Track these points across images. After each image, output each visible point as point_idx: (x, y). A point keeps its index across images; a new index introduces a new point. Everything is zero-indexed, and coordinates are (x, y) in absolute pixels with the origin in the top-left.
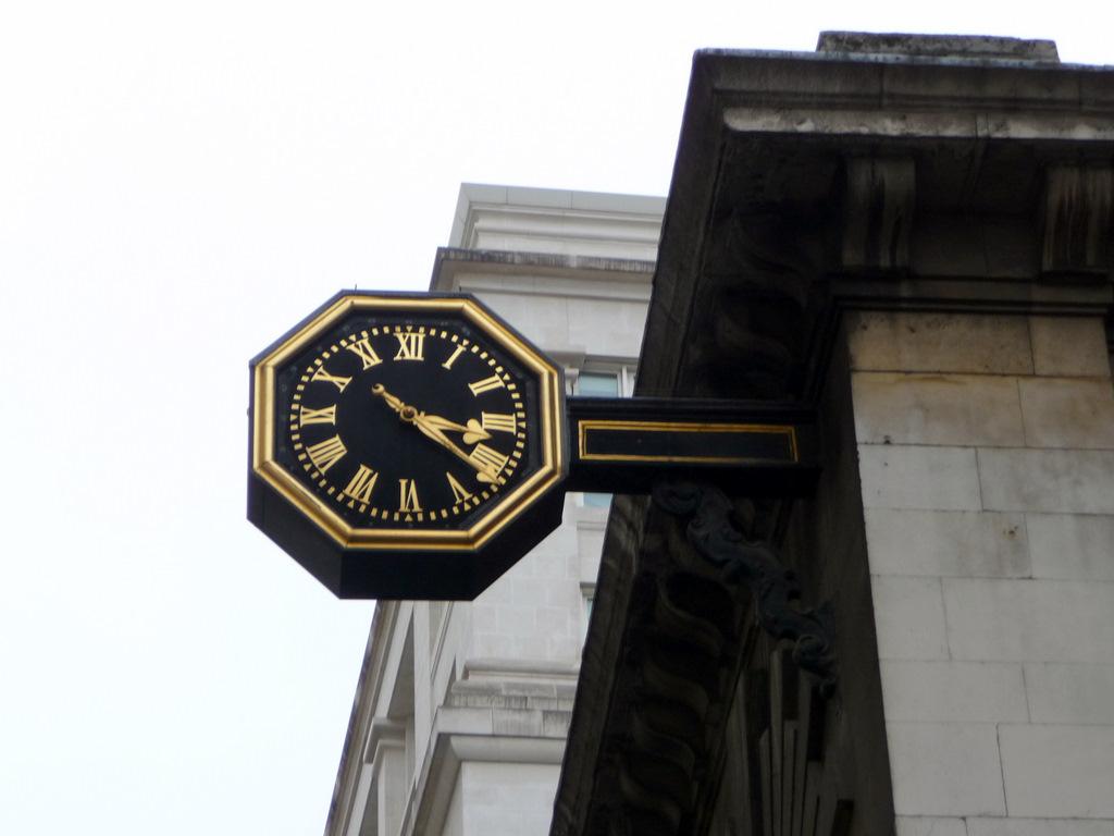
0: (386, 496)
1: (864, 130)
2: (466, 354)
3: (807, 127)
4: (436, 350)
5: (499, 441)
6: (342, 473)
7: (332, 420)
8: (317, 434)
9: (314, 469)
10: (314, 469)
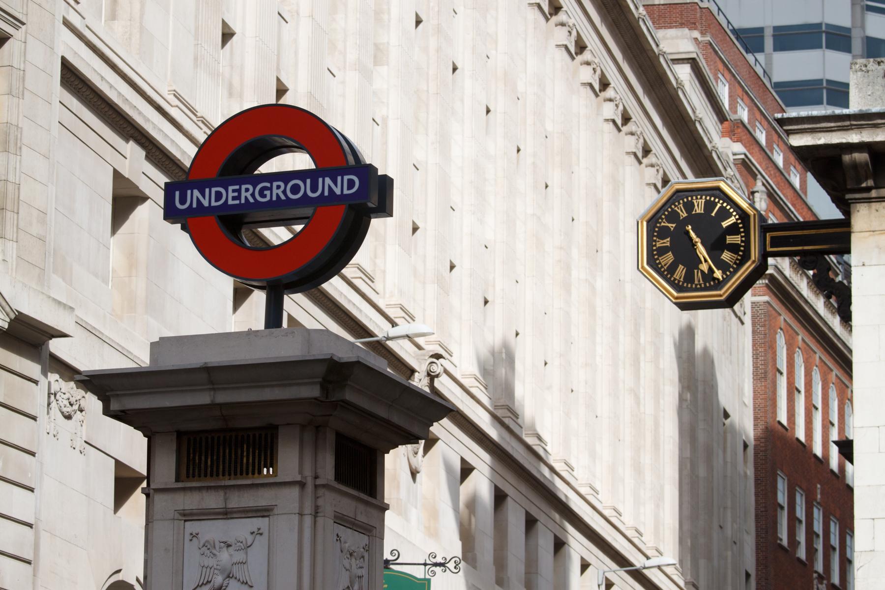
1: (844, 141)
2: (722, 208)
3: (822, 142)
4: (709, 206)
6: (672, 269)
7: (668, 244)
8: (662, 251)
9: (662, 267)
10: (662, 267)
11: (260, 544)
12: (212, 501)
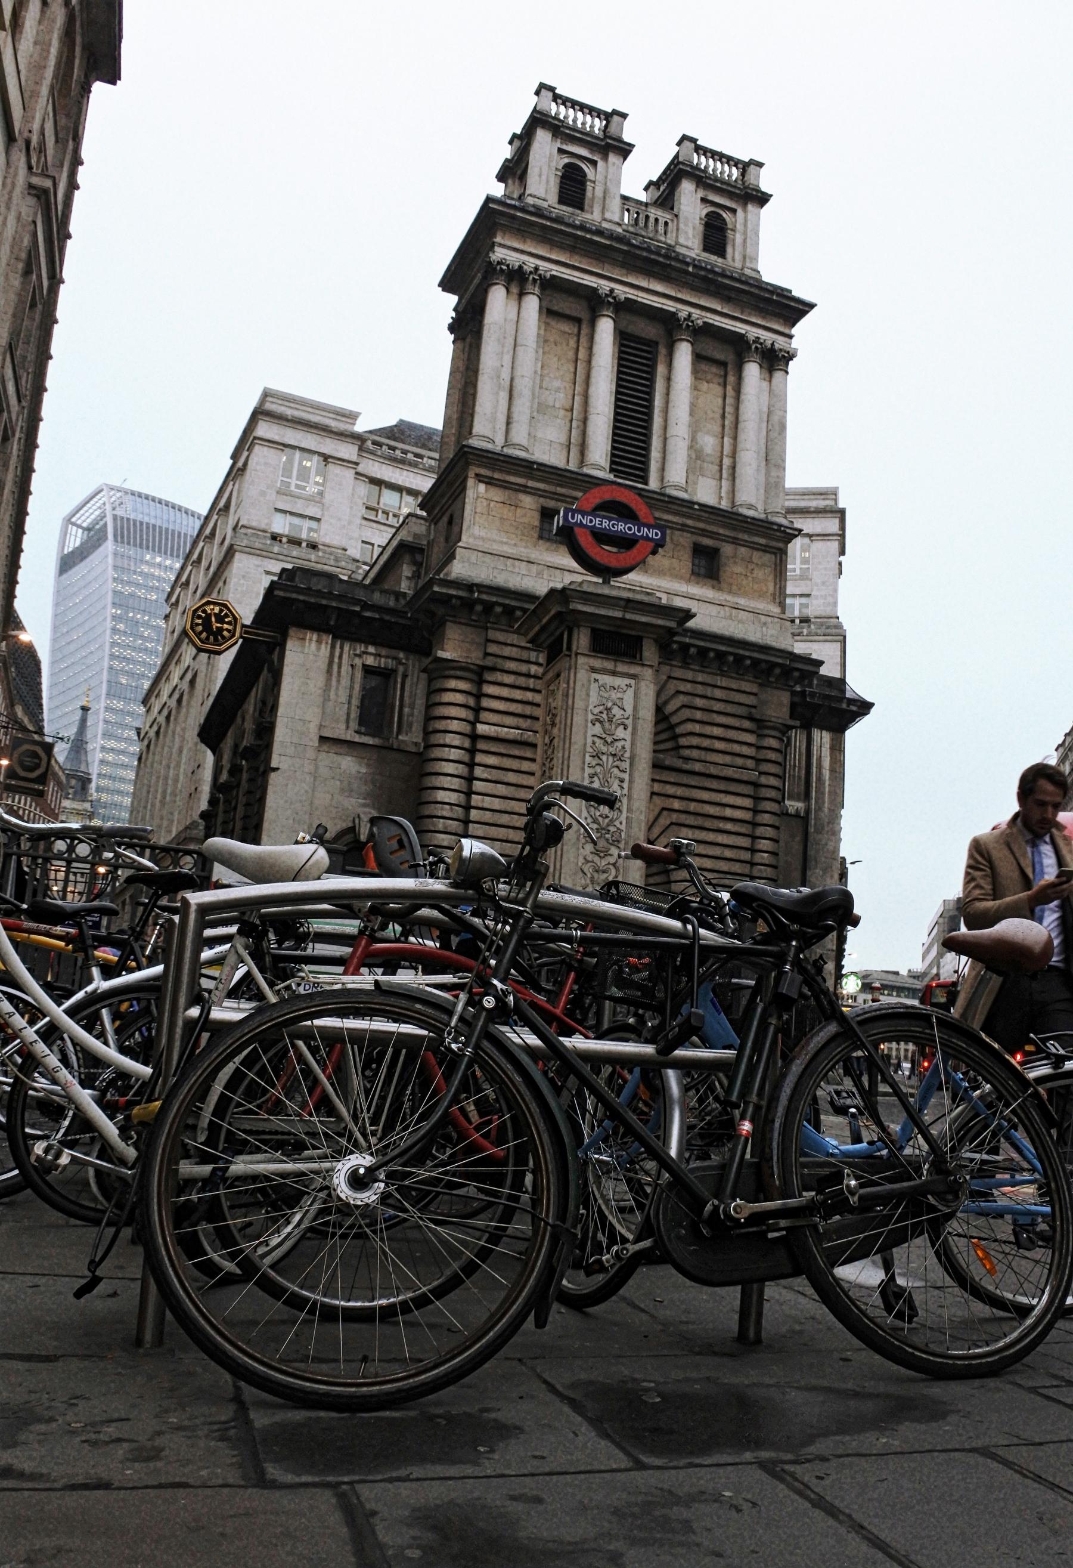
0: (207, 638)
4: (221, 611)
5: (228, 631)
6: (201, 633)
11: (630, 692)
12: (609, 665)
